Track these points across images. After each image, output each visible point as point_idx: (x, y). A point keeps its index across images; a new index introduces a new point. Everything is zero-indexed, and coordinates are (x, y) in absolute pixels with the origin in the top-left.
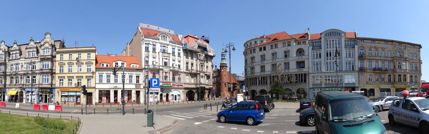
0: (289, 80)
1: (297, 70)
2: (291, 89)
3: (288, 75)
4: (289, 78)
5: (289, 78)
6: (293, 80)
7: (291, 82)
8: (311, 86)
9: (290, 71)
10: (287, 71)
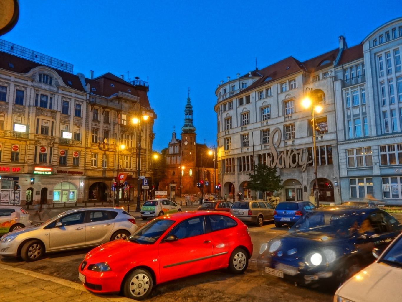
0: (294, 161)
1: (309, 140)
2: (300, 181)
3: (292, 151)
4: (294, 156)
5: (294, 156)
6: (304, 160)
7: (299, 166)
8: (344, 173)
9: (297, 142)
10: (289, 142)
